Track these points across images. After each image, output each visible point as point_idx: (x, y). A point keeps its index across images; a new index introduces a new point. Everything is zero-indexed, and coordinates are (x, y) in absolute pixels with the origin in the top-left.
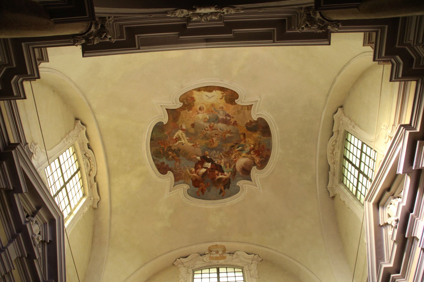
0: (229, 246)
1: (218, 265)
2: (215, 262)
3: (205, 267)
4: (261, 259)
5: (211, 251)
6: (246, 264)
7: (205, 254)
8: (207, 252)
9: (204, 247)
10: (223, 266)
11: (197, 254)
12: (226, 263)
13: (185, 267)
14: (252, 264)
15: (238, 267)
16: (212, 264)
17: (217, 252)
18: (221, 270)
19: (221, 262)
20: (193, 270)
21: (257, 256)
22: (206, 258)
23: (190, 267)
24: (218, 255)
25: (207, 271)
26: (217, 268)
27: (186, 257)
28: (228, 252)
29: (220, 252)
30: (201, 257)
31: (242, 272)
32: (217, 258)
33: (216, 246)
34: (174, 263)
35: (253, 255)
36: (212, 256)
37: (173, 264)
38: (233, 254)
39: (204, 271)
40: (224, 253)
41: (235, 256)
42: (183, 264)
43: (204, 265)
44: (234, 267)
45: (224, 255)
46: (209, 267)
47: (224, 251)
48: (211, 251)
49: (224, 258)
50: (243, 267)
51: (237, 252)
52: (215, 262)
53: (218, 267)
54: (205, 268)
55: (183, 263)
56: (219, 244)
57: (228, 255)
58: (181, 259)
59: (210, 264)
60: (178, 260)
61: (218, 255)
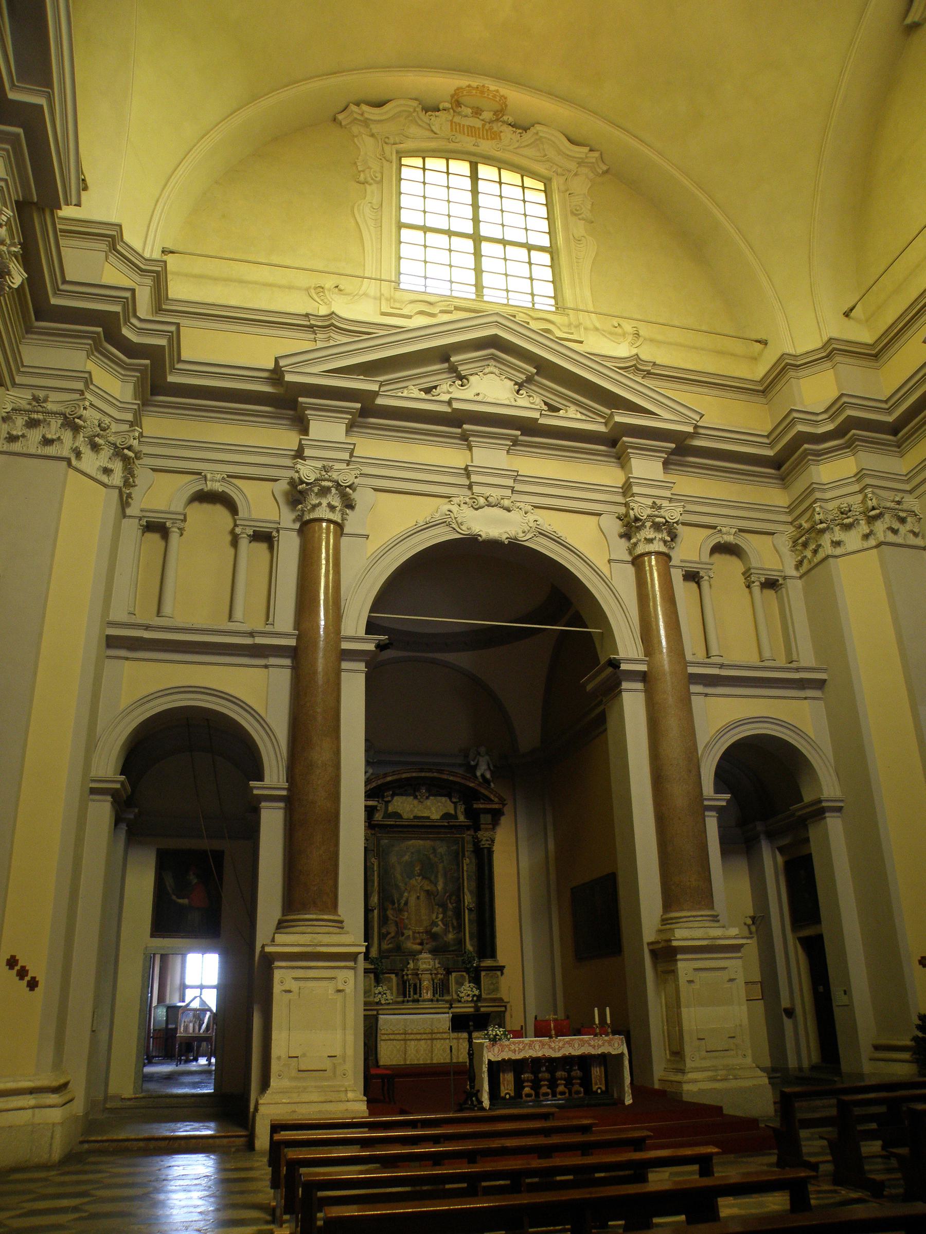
0: (519, 100)
1: (474, 154)
2: (467, 143)
3: (434, 151)
4: (605, 168)
5: (459, 104)
6: (560, 170)
7: (439, 110)
8: (447, 105)
9: (442, 84)
10: (490, 160)
11: (415, 103)
12: (498, 154)
13: (372, 135)
14: (576, 175)
15: (534, 175)
16: (458, 146)
17: (477, 112)
18: (485, 171)
19: (486, 146)
20: (397, 152)
21: (596, 154)
22: (440, 122)
23: (392, 141)
24: (478, 123)
25: (440, 164)
26: (471, 163)
27: (380, 104)
28: (511, 120)
29: (487, 115)
30: (422, 114)
31: (545, 191)
32: (472, 131)
33: (481, 90)
34: (340, 117)
35: (586, 149)
36: (457, 119)
37: (335, 119)
38: (526, 129)
39: (431, 163)
40: (497, 120)
41: (528, 137)
42: (367, 126)
43: (433, 145)
44: (524, 172)
45: (496, 127)
46: (448, 155)
47: (499, 113)
48: (459, 104)
49: (496, 136)
50: (550, 180)
51: (538, 127)
52: (467, 143)
53: (474, 159)
54: (436, 153)
55: (366, 123)
56: (492, 88)
57: (508, 130)
58: (364, 107)
59: (452, 146)
60: (353, 108)
61: (478, 123)
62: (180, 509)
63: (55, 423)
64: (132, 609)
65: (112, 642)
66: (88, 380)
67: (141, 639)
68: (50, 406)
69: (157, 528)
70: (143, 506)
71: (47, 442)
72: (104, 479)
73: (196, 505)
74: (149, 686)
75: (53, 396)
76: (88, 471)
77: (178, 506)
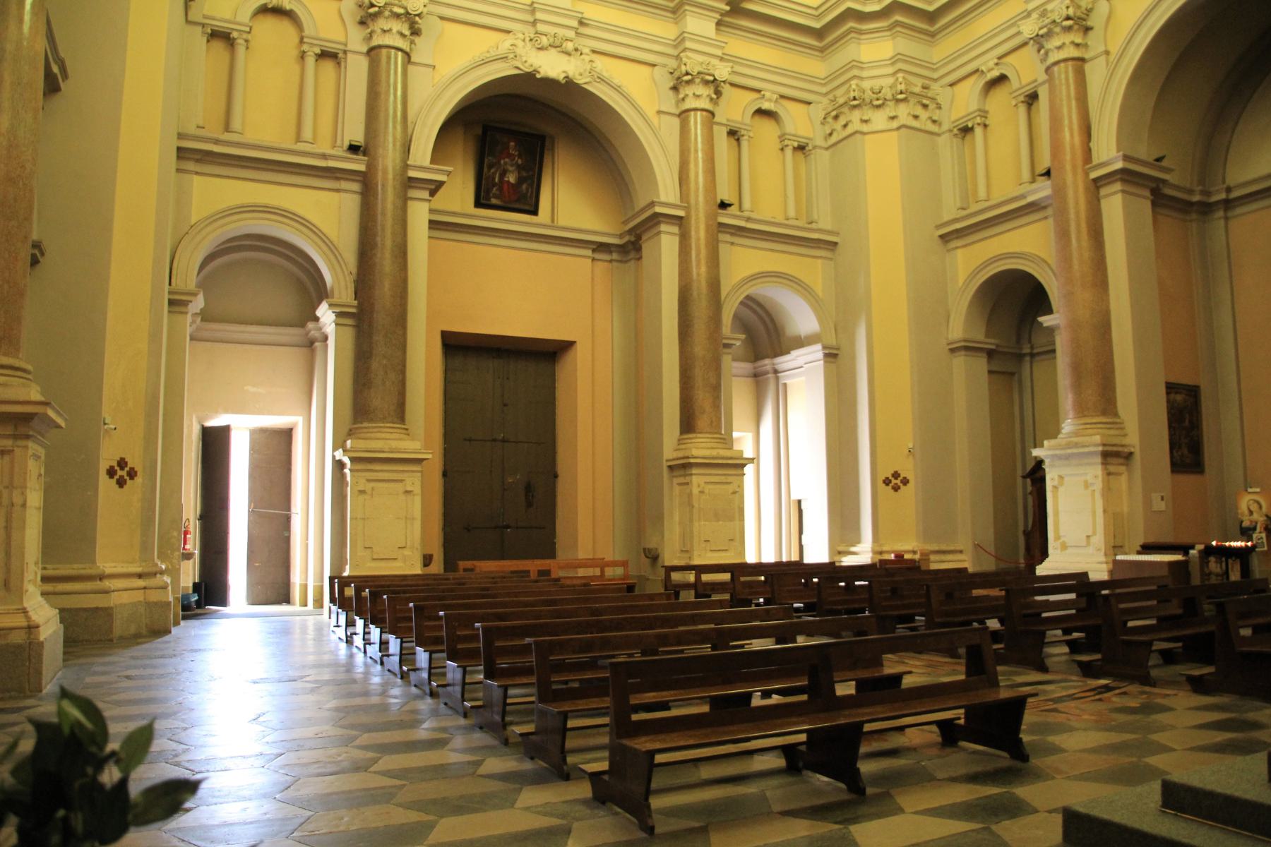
62: (975, 107)
63: (845, 110)
64: (959, 205)
65: (945, 238)
66: (856, 64)
67: (957, 231)
68: (841, 101)
69: (966, 131)
70: (953, 119)
71: (845, 126)
72: (895, 124)
73: (992, 93)
74: (971, 264)
75: (839, 92)
76: (880, 128)
77: (974, 106)
